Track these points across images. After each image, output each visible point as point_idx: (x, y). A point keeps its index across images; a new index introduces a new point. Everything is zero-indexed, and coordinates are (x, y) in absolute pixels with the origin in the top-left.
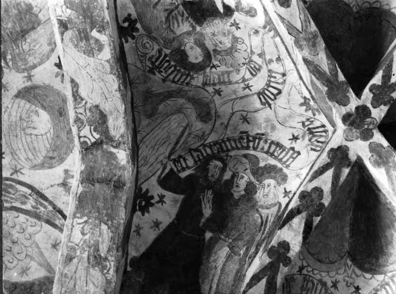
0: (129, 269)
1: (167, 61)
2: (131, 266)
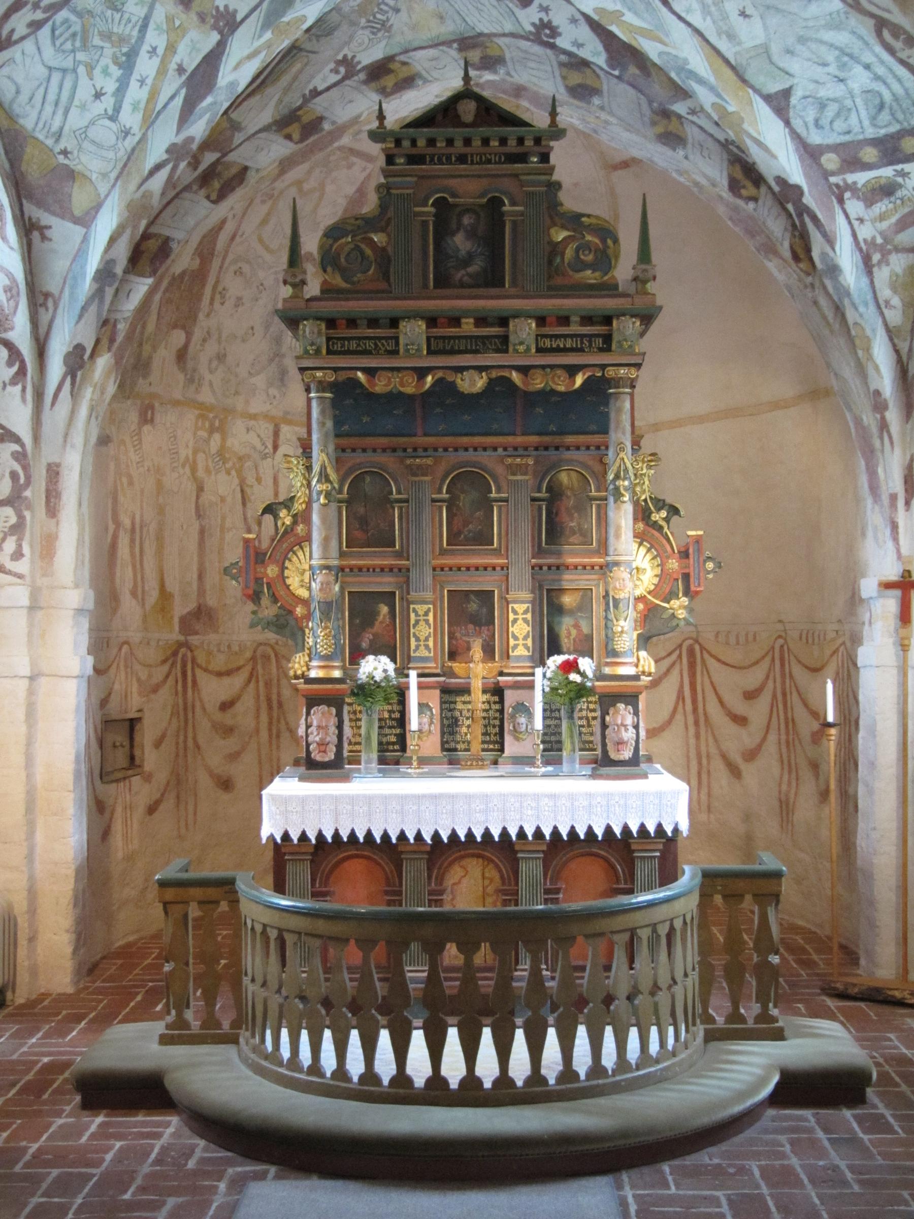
0: (616, 73)
1: (375, 17)
2: (614, 69)
